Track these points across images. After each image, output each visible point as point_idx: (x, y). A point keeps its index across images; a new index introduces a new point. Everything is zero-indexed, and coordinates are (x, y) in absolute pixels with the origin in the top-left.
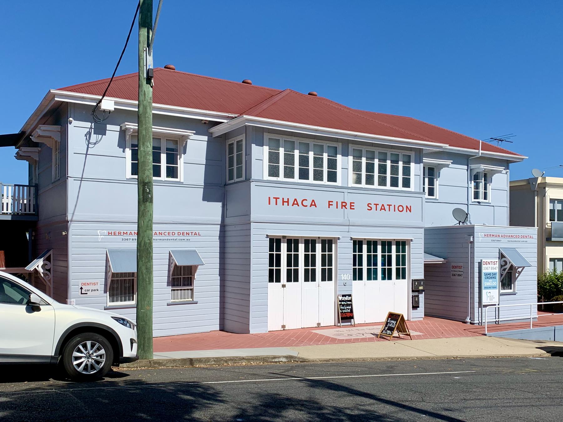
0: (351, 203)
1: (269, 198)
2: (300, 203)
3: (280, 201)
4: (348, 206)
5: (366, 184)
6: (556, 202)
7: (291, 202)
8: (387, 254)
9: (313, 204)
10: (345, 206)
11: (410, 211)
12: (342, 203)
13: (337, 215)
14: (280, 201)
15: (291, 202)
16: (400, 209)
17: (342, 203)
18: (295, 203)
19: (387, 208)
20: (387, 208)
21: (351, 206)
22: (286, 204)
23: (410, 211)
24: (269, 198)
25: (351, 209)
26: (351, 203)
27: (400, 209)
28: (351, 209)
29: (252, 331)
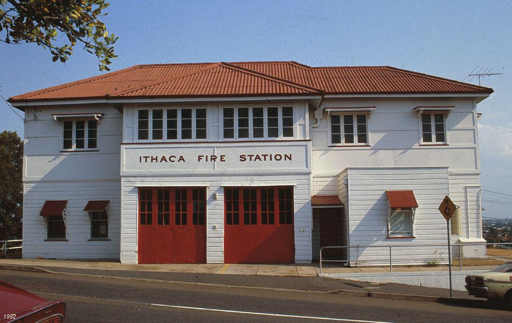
0: (221, 156)
1: (141, 157)
2: (168, 160)
3: (149, 160)
4: (209, 158)
5: (153, 139)
6: (130, 122)
7: (159, 159)
8: (250, 212)
9: (181, 158)
10: (214, 159)
11: (290, 159)
12: (212, 156)
13: (205, 167)
14: (149, 160)
15: (159, 159)
16: (278, 158)
17: (212, 156)
18: (164, 159)
19: (262, 158)
20: (262, 158)
21: (221, 158)
22: (154, 161)
23: (290, 159)
24: (141, 157)
25: (221, 161)
26: (221, 156)
27: (278, 158)
28: (221, 161)
29: (122, 261)
